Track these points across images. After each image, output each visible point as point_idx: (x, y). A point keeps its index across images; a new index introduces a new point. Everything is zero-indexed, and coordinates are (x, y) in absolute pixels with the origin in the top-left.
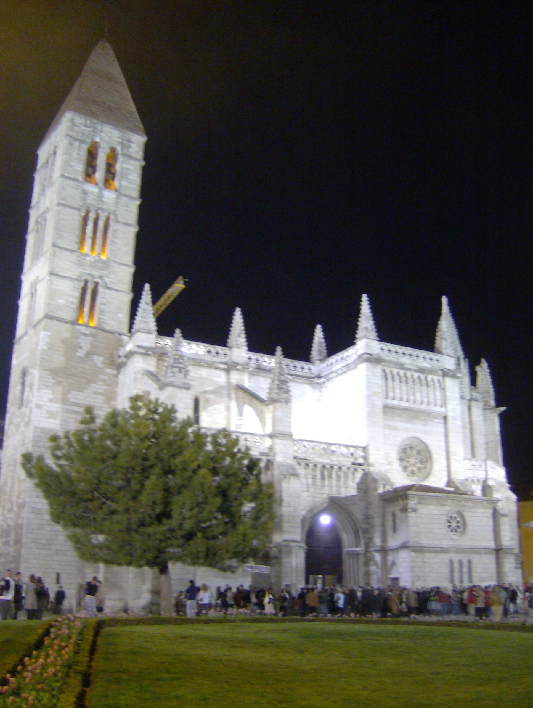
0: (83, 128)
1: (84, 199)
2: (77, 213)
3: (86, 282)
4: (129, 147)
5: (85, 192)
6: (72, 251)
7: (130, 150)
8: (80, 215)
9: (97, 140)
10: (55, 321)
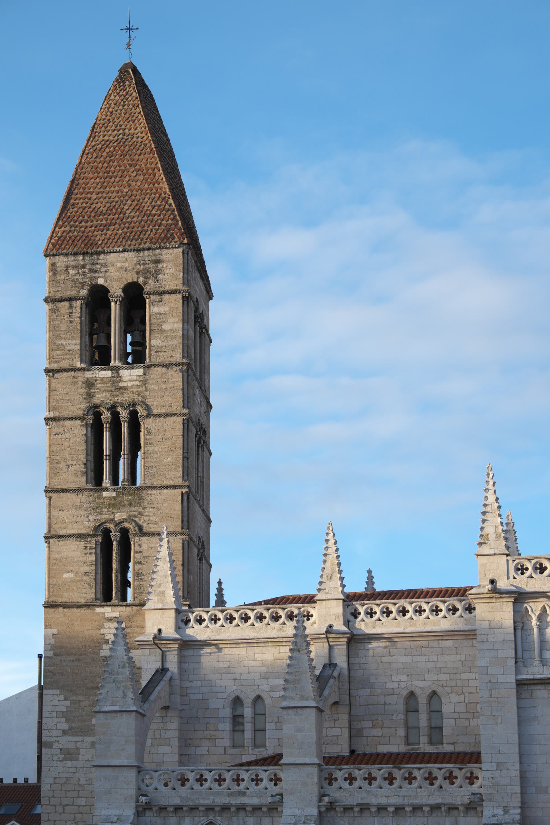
0: (71, 272)
1: (90, 396)
2: (78, 422)
3: (107, 533)
4: (158, 272)
5: (90, 384)
6: (76, 491)
7: (160, 277)
8: (86, 425)
9: (101, 281)
10: (61, 609)
